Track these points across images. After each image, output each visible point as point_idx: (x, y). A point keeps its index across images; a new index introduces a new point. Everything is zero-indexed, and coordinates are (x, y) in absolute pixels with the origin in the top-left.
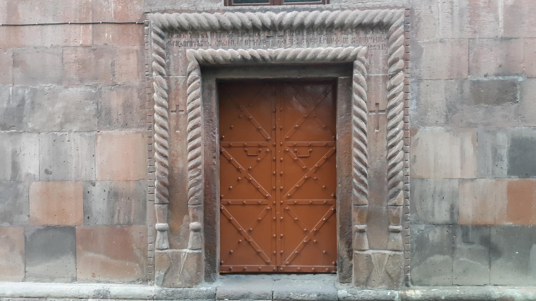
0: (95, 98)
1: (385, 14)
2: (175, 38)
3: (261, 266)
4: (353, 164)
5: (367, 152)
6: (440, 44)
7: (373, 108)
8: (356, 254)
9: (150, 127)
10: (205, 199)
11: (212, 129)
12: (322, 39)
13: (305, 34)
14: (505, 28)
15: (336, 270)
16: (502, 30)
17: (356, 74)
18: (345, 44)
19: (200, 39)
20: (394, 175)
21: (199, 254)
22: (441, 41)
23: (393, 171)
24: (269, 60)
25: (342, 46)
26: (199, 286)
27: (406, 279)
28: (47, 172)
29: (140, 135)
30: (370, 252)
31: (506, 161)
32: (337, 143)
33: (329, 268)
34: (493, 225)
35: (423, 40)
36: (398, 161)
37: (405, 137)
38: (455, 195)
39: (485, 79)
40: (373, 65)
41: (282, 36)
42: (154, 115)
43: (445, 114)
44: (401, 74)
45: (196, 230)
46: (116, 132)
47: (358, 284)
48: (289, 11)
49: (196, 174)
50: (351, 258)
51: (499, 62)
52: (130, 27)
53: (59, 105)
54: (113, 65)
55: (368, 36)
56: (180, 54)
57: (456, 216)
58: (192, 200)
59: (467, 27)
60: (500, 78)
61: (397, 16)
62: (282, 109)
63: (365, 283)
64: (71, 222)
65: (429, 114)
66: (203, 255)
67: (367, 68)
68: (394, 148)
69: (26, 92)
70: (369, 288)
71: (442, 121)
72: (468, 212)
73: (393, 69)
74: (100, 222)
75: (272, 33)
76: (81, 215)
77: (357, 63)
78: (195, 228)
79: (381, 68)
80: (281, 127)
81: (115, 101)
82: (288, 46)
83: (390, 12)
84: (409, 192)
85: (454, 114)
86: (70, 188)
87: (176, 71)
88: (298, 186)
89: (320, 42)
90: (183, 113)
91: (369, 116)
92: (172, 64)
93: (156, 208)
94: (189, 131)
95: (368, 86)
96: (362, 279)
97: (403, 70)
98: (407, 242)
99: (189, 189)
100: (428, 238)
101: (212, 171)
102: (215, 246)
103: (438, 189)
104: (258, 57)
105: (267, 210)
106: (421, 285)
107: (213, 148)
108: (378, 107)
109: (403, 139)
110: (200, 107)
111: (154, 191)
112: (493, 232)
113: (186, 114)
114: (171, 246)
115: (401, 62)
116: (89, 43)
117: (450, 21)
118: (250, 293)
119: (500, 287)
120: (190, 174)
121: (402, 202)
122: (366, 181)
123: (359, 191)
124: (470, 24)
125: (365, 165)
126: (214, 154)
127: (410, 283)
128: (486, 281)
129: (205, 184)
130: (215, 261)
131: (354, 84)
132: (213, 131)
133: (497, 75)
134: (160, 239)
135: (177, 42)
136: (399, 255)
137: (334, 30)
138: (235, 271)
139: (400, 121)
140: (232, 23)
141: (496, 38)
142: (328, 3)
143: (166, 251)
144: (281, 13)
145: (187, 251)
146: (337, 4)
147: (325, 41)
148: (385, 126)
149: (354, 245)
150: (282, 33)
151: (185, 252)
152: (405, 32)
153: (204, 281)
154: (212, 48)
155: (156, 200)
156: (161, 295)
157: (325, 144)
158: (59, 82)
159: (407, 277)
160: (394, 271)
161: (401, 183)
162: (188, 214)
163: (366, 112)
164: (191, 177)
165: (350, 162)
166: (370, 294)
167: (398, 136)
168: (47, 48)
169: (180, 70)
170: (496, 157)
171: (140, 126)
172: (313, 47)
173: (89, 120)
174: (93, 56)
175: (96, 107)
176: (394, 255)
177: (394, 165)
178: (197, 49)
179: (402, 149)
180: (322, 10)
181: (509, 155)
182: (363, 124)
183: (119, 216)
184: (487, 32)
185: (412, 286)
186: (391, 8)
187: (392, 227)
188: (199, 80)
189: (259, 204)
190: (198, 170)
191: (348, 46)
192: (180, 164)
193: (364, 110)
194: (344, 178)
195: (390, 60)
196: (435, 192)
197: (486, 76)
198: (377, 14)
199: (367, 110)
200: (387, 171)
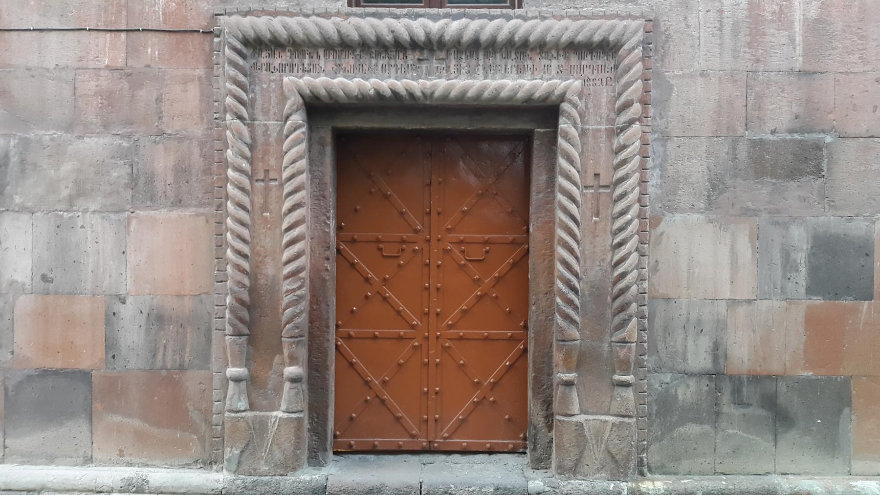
0: (128, 155)
1: (613, 27)
2: (264, 59)
3: (403, 441)
4: (556, 274)
5: (579, 254)
6: (700, 79)
7: (590, 181)
8: (559, 421)
9: (219, 207)
10: (310, 328)
11: (324, 211)
12: (509, 66)
13: (481, 56)
14: (805, 55)
15: (526, 448)
16: (801, 59)
17: (564, 124)
18: (546, 76)
19: (307, 61)
20: (623, 291)
21: (299, 420)
22: (702, 74)
23: (621, 285)
24: (422, 99)
25: (541, 79)
26: (298, 473)
27: (640, 463)
28: (44, 278)
29: (203, 218)
30: (581, 418)
31: (803, 270)
32: (531, 239)
33: (514, 444)
34: (781, 376)
35: (673, 71)
36: (629, 269)
37: (641, 231)
38: (721, 325)
39: (772, 138)
40: (591, 110)
41: (443, 59)
42: (226, 186)
43: (706, 193)
44: (636, 126)
45: (295, 380)
46: (162, 214)
47: (562, 470)
48: (455, 17)
49: (295, 286)
50: (550, 428)
51: (795, 109)
52: (189, 38)
53: (67, 167)
54: (159, 100)
55: (584, 63)
56: (273, 85)
57: (721, 361)
58: (288, 330)
59: (745, 52)
60: (797, 136)
61: (632, 31)
62: (440, 179)
63: (573, 470)
64: (85, 364)
65: (680, 192)
66: (306, 422)
67: (581, 116)
68: (623, 247)
69: (12, 143)
70: (580, 477)
71: (701, 204)
72: (741, 354)
73: (623, 118)
74: (132, 365)
75: (426, 53)
76: (101, 353)
77: (565, 106)
78: (293, 376)
79: (604, 115)
80: (440, 210)
81: (162, 162)
82: (453, 75)
83: (620, 24)
84: (646, 321)
85: (721, 193)
86: (84, 307)
87: (266, 113)
88: (465, 307)
89: (506, 71)
90: (276, 183)
91: (583, 195)
92: (259, 102)
93: (228, 343)
94: (286, 215)
95: (583, 144)
96: (569, 464)
97: (639, 120)
98: (642, 402)
99: (284, 310)
100: (676, 395)
101: (324, 281)
102: (327, 407)
103: (694, 316)
104: (403, 93)
105: (414, 347)
106: (664, 474)
107: (325, 242)
109: (637, 233)
110: (305, 174)
111: (224, 314)
112: (782, 387)
113: (282, 185)
114: (252, 407)
115: (637, 106)
116: (120, 63)
117: (718, 42)
118: (383, 485)
119: (791, 477)
120: (286, 286)
121: (635, 337)
122: (577, 302)
123: (566, 317)
124: (750, 48)
125: (576, 275)
126: (328, 253)
127: (646, 470)
128: (770, 467)
129: (311, 303)
130: (325, 431)
131: (561, 141)
132: (325, 215)
133: (791, 131)
134: (233, 395)
135: (268, 65)
136: (628, 424)
137: (528, 52)
138: (359, 449)
139: (634, 204)
140: (360, 36)
141: (790, 72)
142: (520, 7)
143: (244, 414)
144: (442, 22)
145: (279, 414)
146: (534, 8)
147: (514, 69)
148: (609, 211)
149: (556, 406)
150: (443, 55)
151: (276, 417)
152: (645, 58)
153: (306, 465)
154: (326, 75)
155: (229, 329)
156: (234, 487)
157: (511, 239)
158: (69, 128)
159: (642, 459)
160: (621, 449)
161: (634, 305)
162: (282, 353)
164: (287, 291)
165: (551, 268)
166: (581, 487)
167: (630, 228)
168: (48, 69)
169: (272, 112)
170: (789, 265)
171: (201, 205)
172: (494, 79)
173: (118, 193)
174: (126, 86)
175: (129, 171)
176: (621, 423)
177: (623, 275)
178: (301, 77)
179: (637, 250)
180: (509, 18)
181: (809, 262)
182: (573, 208)
183: (164, 354)
184: (776, 61)
185: (649, 475)
186: (622, 18)
187: (617, 377)
188: (304, 129)
189: (400, 338)
190: (300, 279)
191: (551, 79)
192: (269, 270)
193: (575, 184)
194: (541, 296)
195: (618, 104)
196: (688, 320)
197: (773, 132)
198: (599, 28)
200: (611, 285)
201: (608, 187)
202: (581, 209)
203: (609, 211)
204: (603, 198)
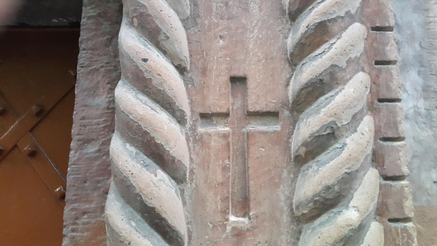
7: (218, 97)
91: (196, 141)
108: (245, 96)
148: (282, 192)
163: (181, 121)
193: (167, 104)
199: (183, 101)
201: (272, 115)
202: (189, 187)
203: (282, 192)
204: (257, 151)
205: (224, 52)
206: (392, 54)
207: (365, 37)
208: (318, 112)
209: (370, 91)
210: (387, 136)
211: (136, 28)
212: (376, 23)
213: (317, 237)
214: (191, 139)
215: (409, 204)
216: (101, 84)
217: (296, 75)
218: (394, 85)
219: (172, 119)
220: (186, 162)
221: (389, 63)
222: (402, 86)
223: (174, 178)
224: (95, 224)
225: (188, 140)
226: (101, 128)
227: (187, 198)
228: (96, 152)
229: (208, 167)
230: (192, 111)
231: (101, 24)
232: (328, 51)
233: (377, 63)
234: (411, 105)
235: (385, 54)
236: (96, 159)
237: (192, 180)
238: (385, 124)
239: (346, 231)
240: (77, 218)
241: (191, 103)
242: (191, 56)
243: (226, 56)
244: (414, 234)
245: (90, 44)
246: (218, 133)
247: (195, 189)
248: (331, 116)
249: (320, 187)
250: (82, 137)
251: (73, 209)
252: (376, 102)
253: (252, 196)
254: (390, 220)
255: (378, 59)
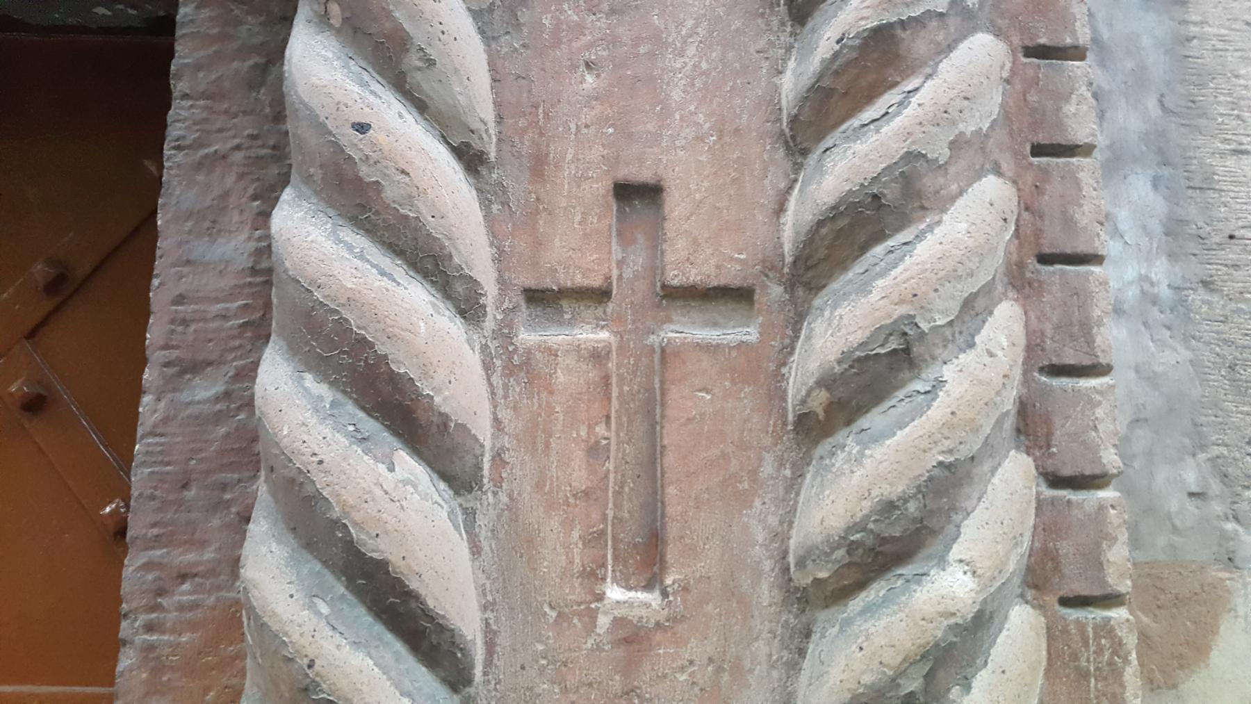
7: (579, 244)
91: (512, 368)
108: (656, 240)
139: (990, 450)
148: (758, 520)
163: (468, 307)
193: (427, 260)
199: (474, 250)
201: (735, 296)
202: (488, 503)
203: (758, 520)
204: (691, 401)
205: (598, 108)
206: (1080, 122)
207: (1005, 74)
208: (864, 289)
209: (1016, 230)
210: (1061, 362)
211: (338, 31)
212: (1037, 36)
213: (854, 647)
214: (498, 362)
215: (1118, 555)
216: (233, 200)
217: (806, 184)
218: (1084, 216)
219: (441, 305)
220: (483, 430)
221: (1070, 150)
222: (1106, 220)
223: (445, 476)
224: (214, 608)
225: (488, 367)
226: (231, 328)
227: (484, 534)
228: (217, 399)
229: (547, 445)
230: (502, 282)
231: (238, 23)
232: (898, 114)
233: (1038, 150)
234: (1131, 273)
235: (1060, 126)
236: (218, 418)
237: (498, 482)
238: (1057, 328)
239: (937, 631)
240: (161, 592)
241: (500, 257)
242: (500, 119)
243: (604, 121)
244: (1131, 641)
245: (204, 79)
246: (577, 348)
247: (509, 508)
248: (901, 302)
249: (867, 505)
250: (175, 354)
251: (148, 566)
252: (1032, 262)
253: (673, 530)
254: (1066, 602)
255: (1042, 138)
